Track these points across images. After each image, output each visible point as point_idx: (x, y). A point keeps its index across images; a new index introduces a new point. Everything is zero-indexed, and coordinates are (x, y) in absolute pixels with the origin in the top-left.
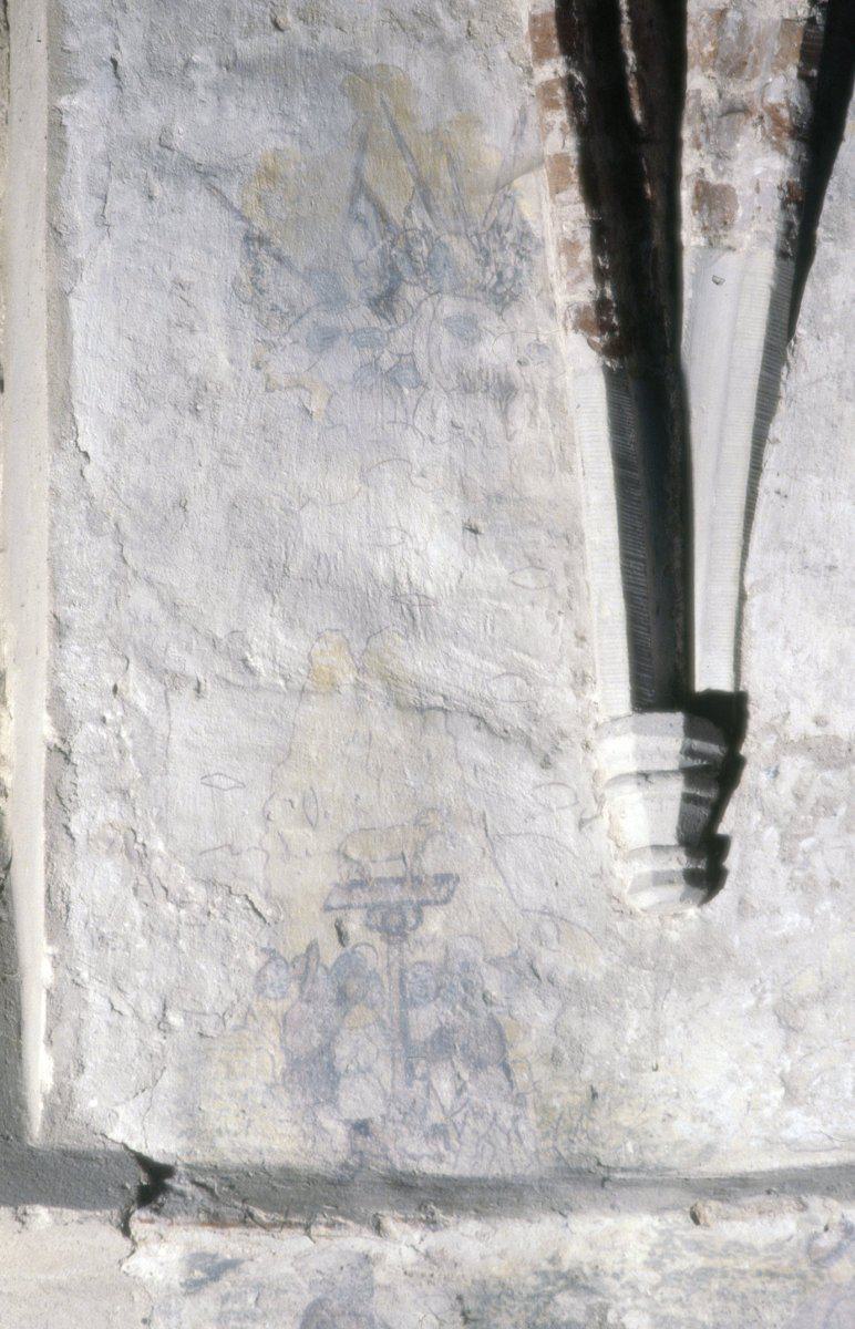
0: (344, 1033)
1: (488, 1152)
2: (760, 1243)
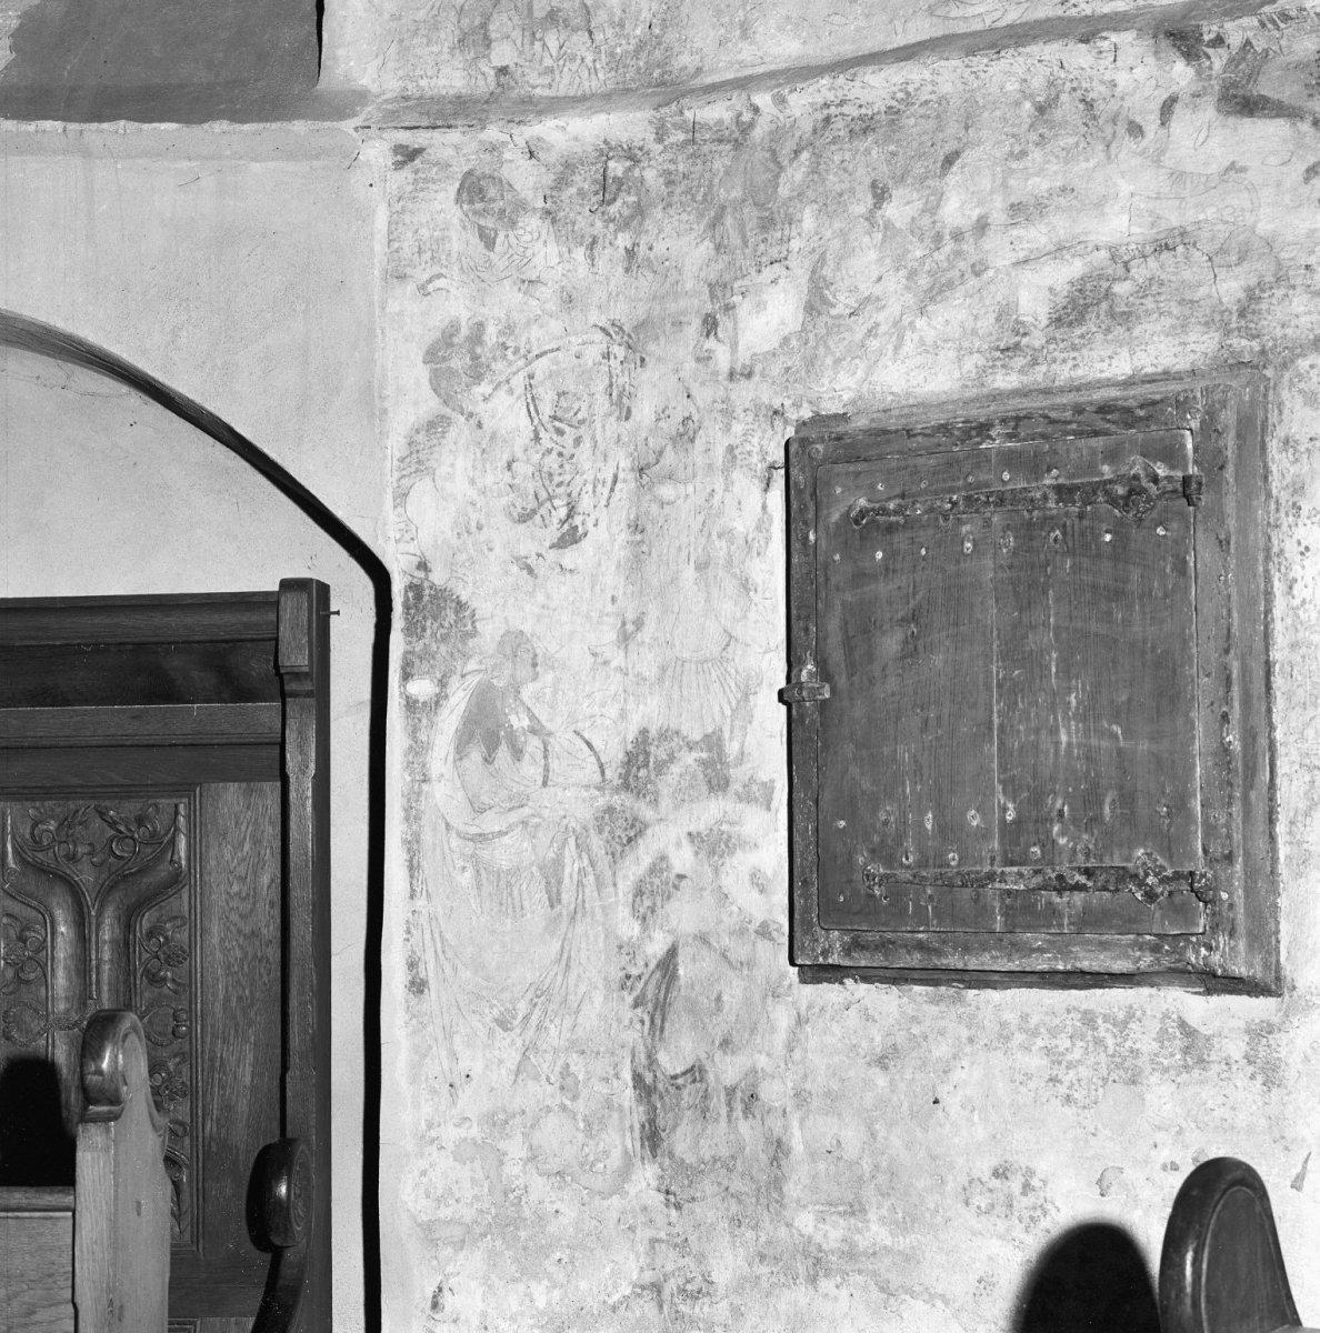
0: (495, 15)
1: (577, 80)
2: (711, 123)
